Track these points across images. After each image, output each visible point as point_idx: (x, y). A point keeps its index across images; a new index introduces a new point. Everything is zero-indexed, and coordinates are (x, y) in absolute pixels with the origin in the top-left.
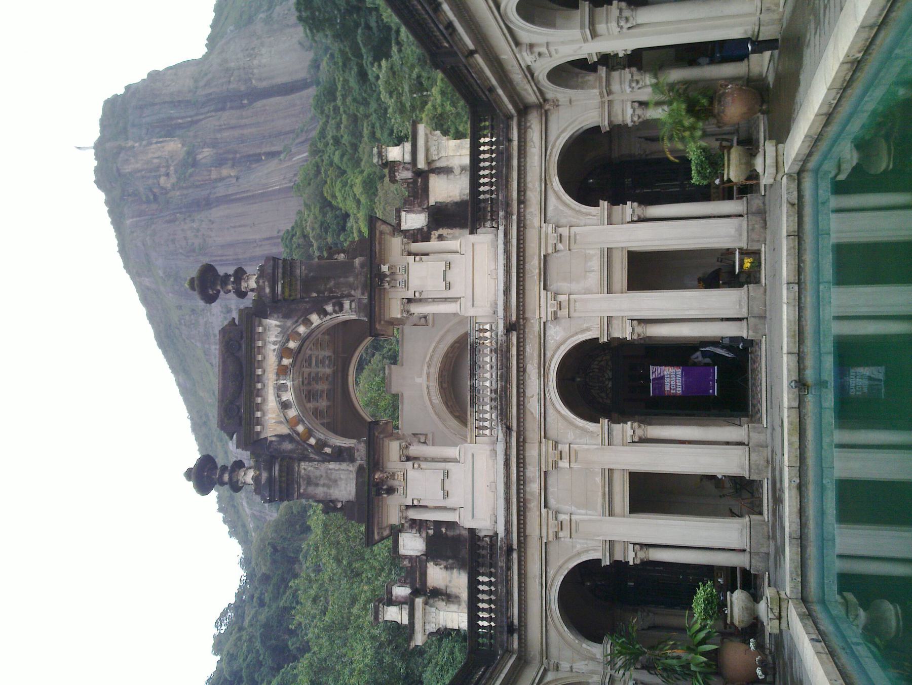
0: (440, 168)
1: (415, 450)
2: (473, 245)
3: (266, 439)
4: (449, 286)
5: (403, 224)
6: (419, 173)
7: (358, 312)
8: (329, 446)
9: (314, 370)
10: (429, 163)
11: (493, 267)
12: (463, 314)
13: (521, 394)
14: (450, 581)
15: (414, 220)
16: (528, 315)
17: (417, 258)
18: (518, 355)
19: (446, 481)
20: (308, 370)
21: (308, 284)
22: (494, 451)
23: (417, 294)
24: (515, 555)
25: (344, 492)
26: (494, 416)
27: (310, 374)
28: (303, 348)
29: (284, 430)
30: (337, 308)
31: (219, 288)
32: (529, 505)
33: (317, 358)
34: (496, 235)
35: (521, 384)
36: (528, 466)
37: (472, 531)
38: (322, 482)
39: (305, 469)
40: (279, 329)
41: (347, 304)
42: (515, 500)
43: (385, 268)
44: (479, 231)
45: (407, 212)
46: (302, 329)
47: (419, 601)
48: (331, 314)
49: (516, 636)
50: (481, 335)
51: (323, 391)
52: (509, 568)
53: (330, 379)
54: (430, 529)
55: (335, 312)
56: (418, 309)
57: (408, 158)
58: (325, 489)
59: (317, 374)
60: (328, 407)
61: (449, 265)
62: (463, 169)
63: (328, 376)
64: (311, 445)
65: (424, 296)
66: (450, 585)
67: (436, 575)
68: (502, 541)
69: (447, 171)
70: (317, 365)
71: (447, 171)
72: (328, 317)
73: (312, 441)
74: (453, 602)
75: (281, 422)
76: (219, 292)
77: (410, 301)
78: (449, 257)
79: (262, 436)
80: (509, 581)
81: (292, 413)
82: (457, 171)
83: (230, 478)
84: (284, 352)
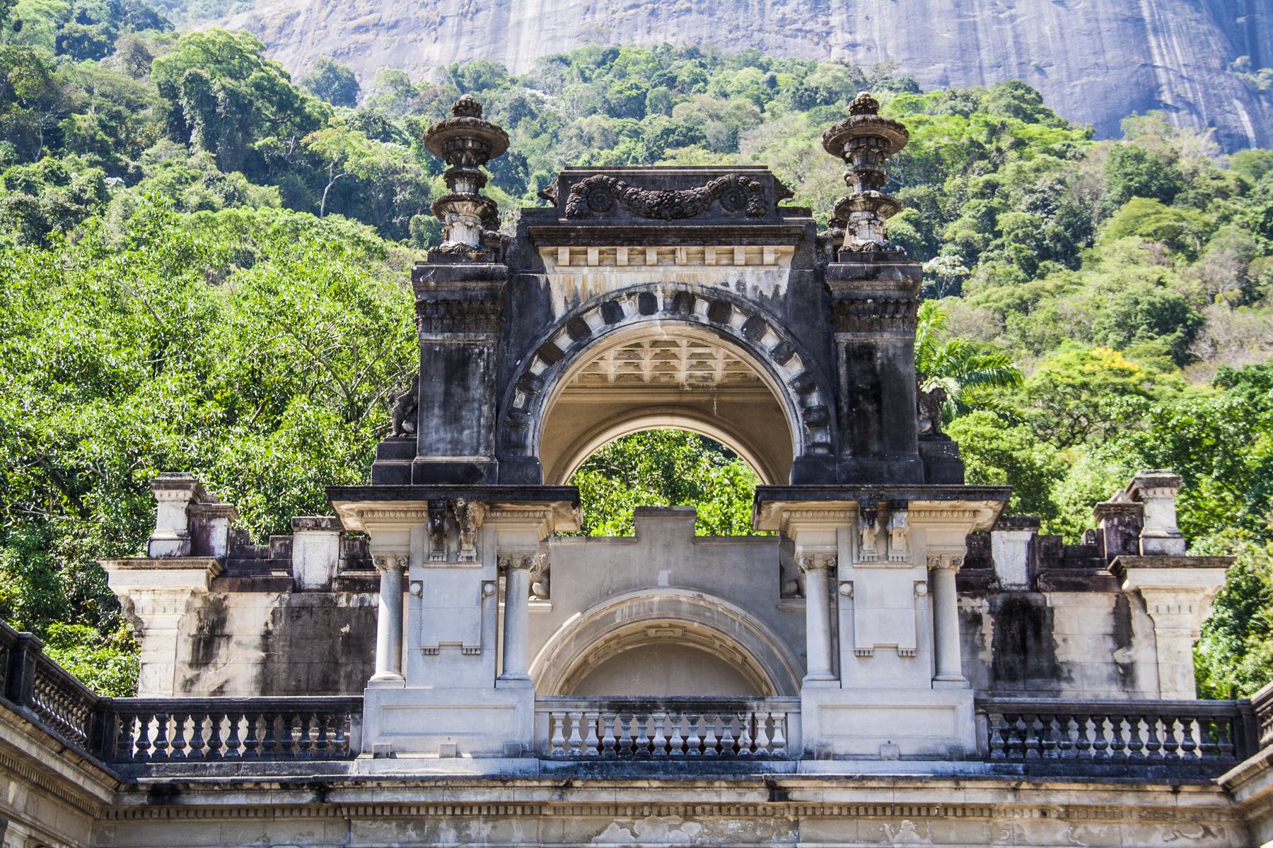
0: (1129, 617)
1: (522, 577)
2: (953, 708)
3: (542, 270)
4: (863, 655)
5: (1004, 533)
6: (1119, 574)
7: (807, 459)
8: (528, 401)
9: (684, 351)
10: (1137, 593)
11: (907, 749)
12: (805, 685)
13: (638, 810)
14: (239, 644)
15: (1011, 557)
16: (805, 829)
17: (923, 589)
18: (720, 805)
19: (458, 652)
20: (684, 343)
21: (863, 354)
22: (516, 752)
23: (845, 589)
24: (308, 797)
25: (434, 437)
26: (593, 751)
27: (674, 344)
28: (730, 345)
29: (559, 310)
30: (815, 416)
31: (857, 162)
32: (410, 826)
33: (711, 356)
34: (971, 757)
35: (658, 810)
36: (490, 824)
37: (356, 707)
38: (457, 390)
39: (481, 352)
40: (770, 295)
41: (821, 437)
42: (422, 797)
43: (900, 520)
44: (983, 720)
45: (1032, 546)
46: (770, 341)
47: (197, 579)
48: (802, 403)
49: (145, 800)
50: (761, 725)
51: (637, 366)
52: (285, 786)
53: (664, 379)
54: (348, 600)
55: (808, 411)
56: (813, 584)
57: (1154, 545)
58: (442, 398)
59: (675, 356)
60: (604, 378)
61: (909, 655)
62: (1126, 674)
63: (672, 376)
64: (529, 365)
65: (843, 604)
66: (232, 645)
67: (252, 613)
68: (334, 769)
69: (1122, 634)
70: (693, 356)
71: (1122, 634)
72: (795, 399)
73: (538, 368)
74: (195, 650)
75: (576, 303)
76: (849, 161)
77: (832, 571)
78: (927, 655)
79: (547, 262)
80: (258, 788)
81: (595, 321)
82: (1122, 656)
83: (460, 199)
84: (720, 306)
